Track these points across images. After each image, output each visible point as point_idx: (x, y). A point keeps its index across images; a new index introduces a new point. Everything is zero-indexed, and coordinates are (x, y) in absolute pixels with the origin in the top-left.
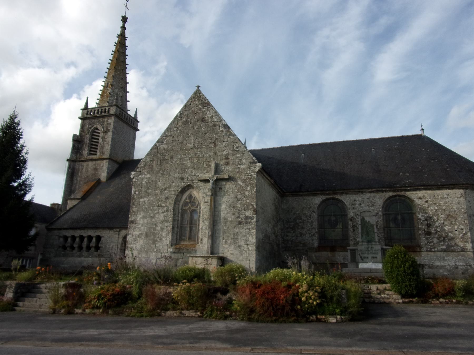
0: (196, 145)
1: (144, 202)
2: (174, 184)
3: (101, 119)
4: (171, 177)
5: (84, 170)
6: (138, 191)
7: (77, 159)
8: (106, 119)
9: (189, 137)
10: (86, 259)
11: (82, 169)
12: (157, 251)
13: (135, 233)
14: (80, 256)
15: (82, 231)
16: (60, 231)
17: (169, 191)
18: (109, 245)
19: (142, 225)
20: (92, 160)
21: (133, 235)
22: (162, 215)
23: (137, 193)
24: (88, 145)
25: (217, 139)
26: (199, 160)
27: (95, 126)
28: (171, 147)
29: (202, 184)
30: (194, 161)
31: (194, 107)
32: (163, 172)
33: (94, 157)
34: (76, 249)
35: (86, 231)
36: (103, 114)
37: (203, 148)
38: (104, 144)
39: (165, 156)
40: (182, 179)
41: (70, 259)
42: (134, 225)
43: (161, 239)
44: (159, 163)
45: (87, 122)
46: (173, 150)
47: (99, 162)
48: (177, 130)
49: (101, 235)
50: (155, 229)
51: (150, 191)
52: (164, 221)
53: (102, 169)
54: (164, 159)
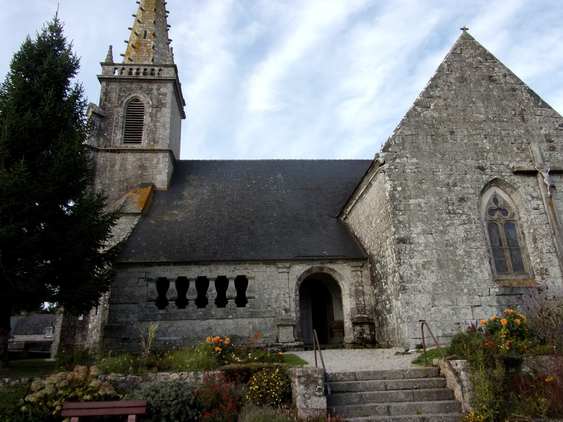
0: (491, 116)
1: (420, 205)
2: (468, 176)
3: (144, 85)
4: (459, 165)
5: (117, 167)
6: (401, 185)
7: (98, 146)
8: (155, 86)
9: (474, 103)
10: (221, 322)
11: (113, 166)
12: (469, 294)
13: (413, 262)
14: (205, 317)
15: (203, 268)
16: (148, 269)
17: (464, 188)
18: (270, 294)
19: (426, 246)
20: (133, 151)
21: (411, 265)
22: (461, 228)
23: (399, 189)
24: (120, 124)
25: (524, 110)
26: (502, 139)
27: (133, 95)
28: (445, 115)
29: (517, 179)
30: (494, 141)
31: (469, 57)
32: (443, 155)
33: (137, 146)
34: (192, 303)
35: (213, 267)
36: (149, 77)
37: (503, 121)
38: (155, 126)
39: (438, 129)
40: (482, 169)
41: (180, 323)
42: (408, 246)
43: (471, 271)
44: (430, 140)
45: (114, 86)
46: (450, 120)
47: (148, 155)
48: (449, 90)
49: (248, 275)
50: (454, 254)
51: (424, 187)
52: (467, 239)
53: (156, 167)
54: (437, 135)
